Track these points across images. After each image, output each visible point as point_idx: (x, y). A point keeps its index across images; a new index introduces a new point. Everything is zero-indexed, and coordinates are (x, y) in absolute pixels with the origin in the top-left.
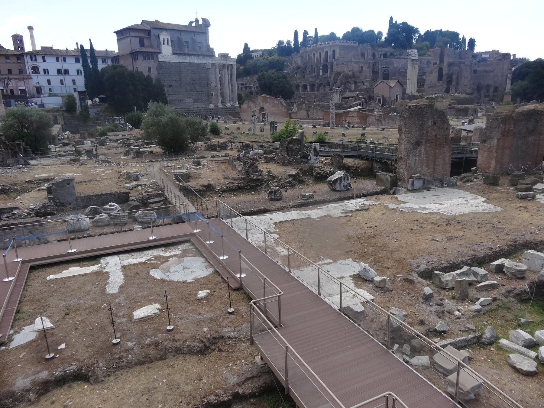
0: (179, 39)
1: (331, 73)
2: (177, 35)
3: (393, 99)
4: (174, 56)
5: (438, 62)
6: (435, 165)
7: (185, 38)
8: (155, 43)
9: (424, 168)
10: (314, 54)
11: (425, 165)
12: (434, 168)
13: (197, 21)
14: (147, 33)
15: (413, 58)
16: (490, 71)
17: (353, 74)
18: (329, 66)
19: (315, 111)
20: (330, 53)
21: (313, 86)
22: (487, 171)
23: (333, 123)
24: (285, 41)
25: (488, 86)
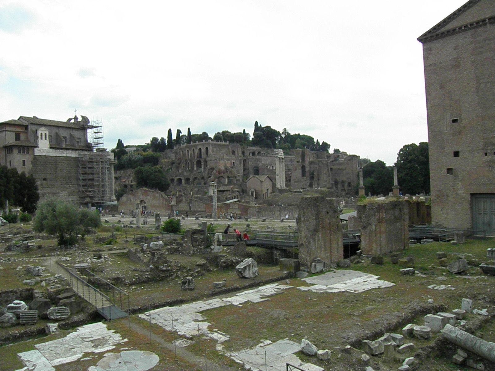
0: (57, 135)
1: (205, 169)
2: (55, 130)
3: (264, 192)
4: (51, 150)
5: (300, 161)
6: (331, 249)
7: (63, 133)
8: (32, 139)
9: (323, 252)
10: (188, 150)
11: (323, 249)
12: (331, 252)
13: (76, 118)
14: (24, 129)
15: (280, 157)
16: (343, 169)
17: (226, 169)
18: (202, 162)
19: (197, 203)
20: (203, 151)
21: (187, 180)
22: (370, 253)
23: (215, 215)
24: (160, 138)
25: (343, 182)
